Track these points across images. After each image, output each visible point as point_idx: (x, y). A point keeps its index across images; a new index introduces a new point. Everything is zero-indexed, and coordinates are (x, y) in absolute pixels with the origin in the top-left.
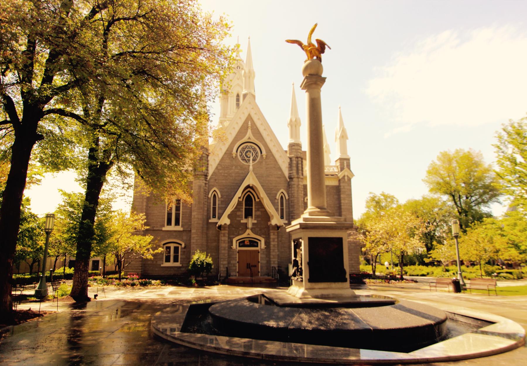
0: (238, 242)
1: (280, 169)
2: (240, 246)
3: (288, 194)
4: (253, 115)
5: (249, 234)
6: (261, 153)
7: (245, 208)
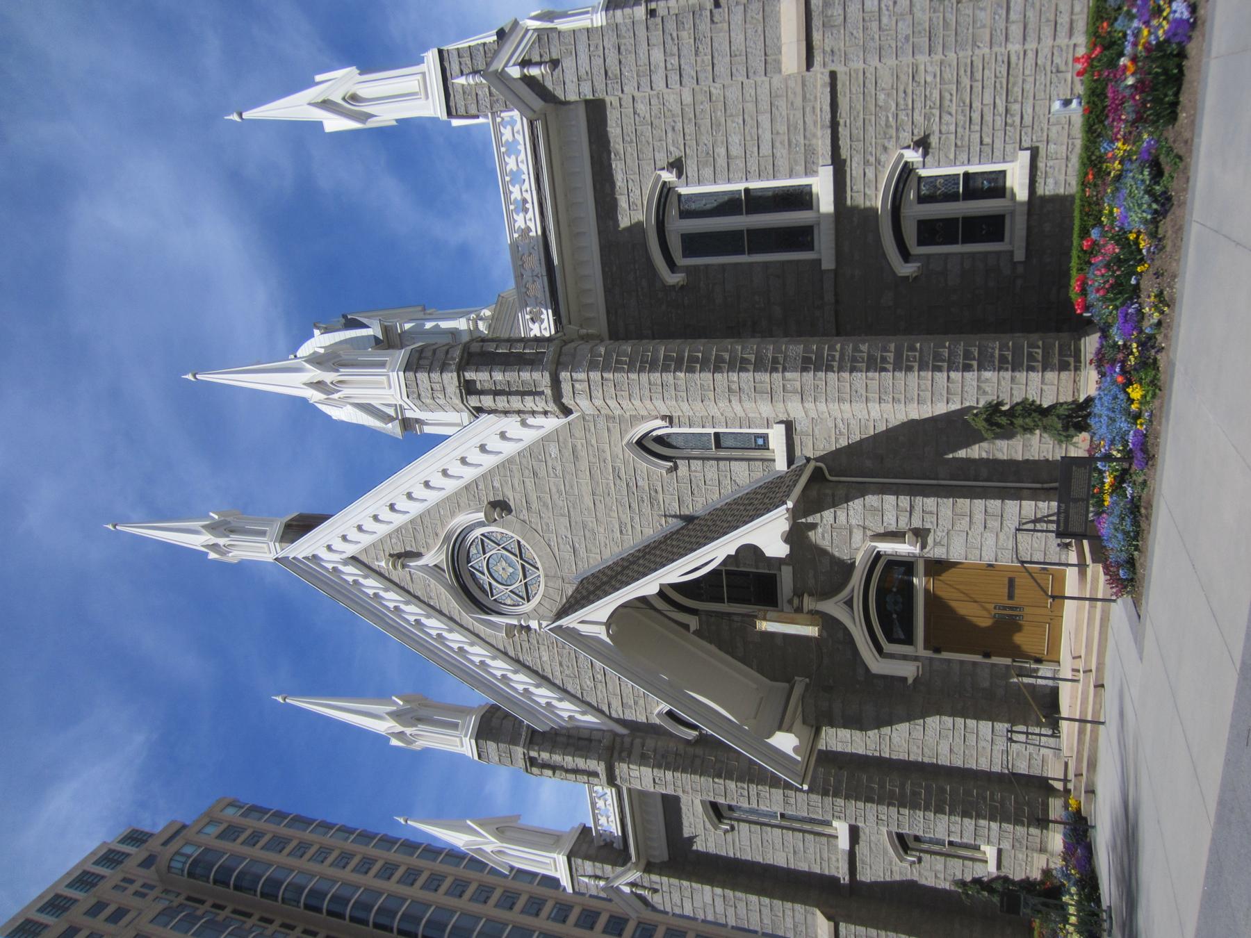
0: (889, 647)
1: (535, 452)
2: (909, 640)
3: (643, 419)
4: (351, 550)
5: (849, 603)
6: (481, 524)
7: (732, 600)
